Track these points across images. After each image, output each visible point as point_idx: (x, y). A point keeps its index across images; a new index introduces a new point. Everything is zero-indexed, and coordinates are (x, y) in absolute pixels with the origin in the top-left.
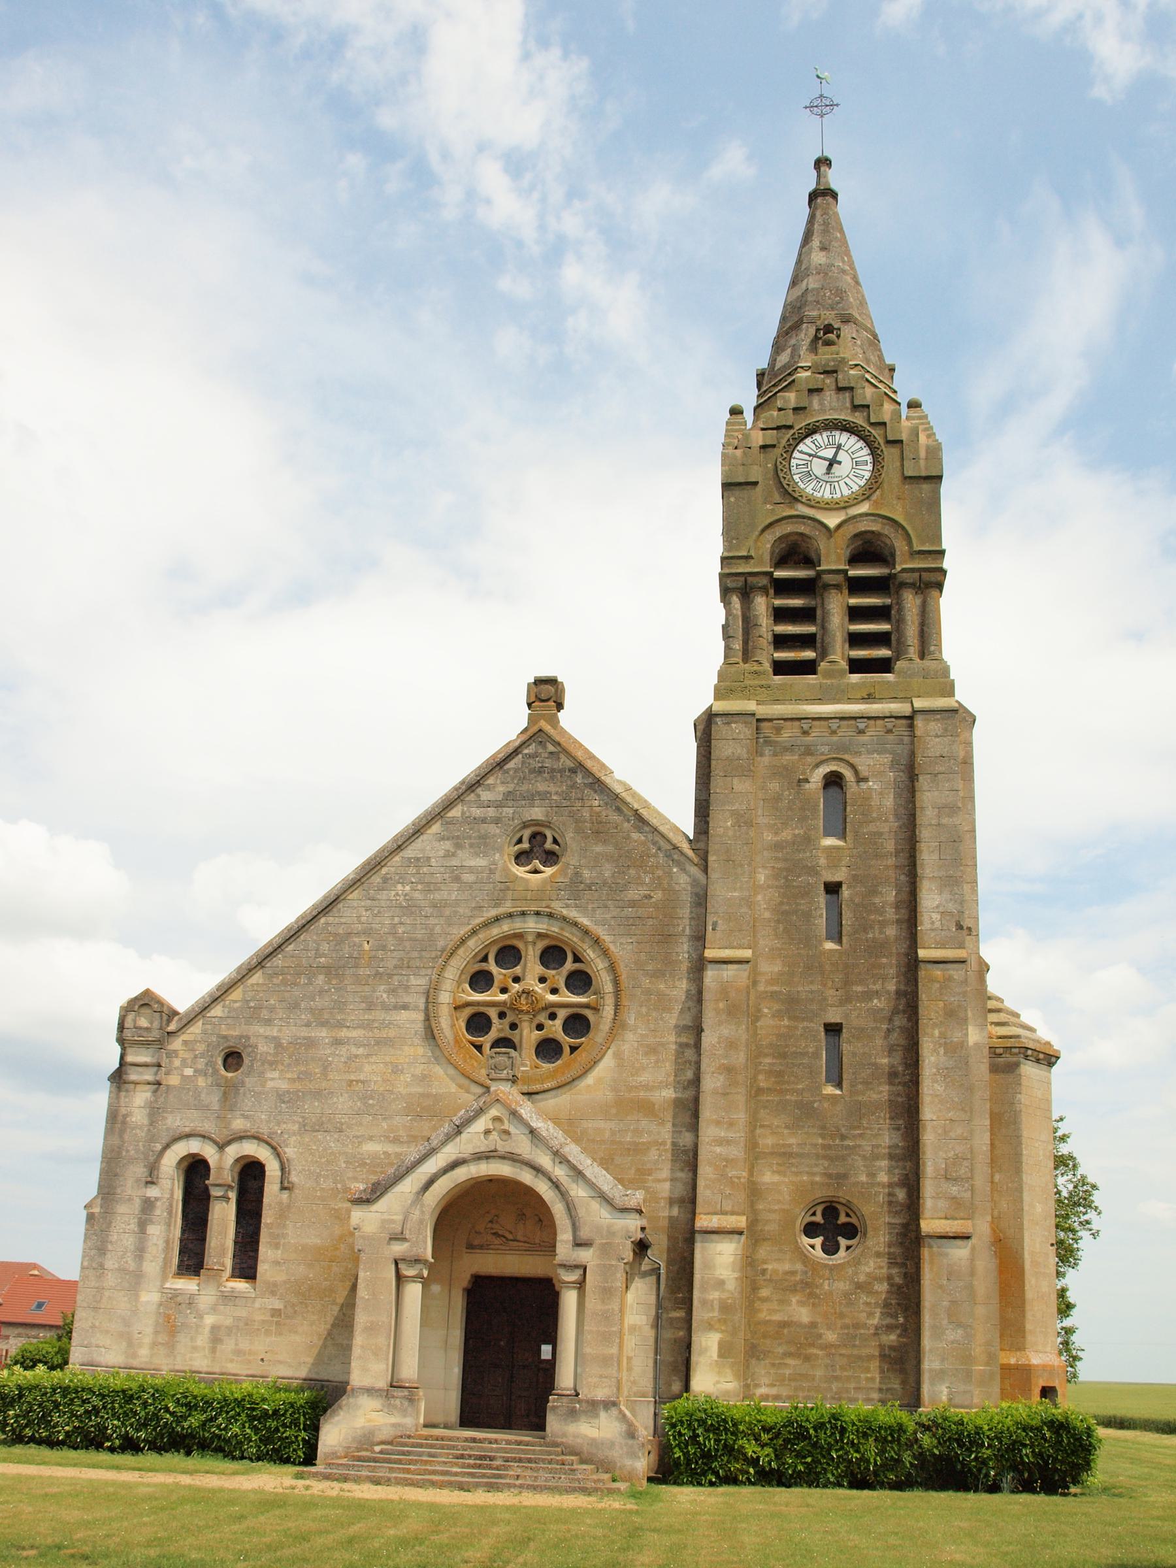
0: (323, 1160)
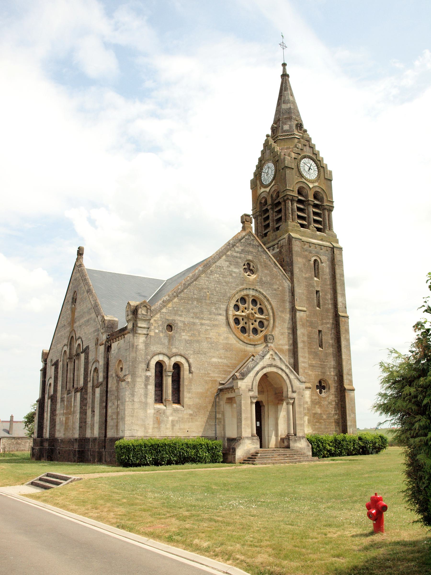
0: (201, 364)
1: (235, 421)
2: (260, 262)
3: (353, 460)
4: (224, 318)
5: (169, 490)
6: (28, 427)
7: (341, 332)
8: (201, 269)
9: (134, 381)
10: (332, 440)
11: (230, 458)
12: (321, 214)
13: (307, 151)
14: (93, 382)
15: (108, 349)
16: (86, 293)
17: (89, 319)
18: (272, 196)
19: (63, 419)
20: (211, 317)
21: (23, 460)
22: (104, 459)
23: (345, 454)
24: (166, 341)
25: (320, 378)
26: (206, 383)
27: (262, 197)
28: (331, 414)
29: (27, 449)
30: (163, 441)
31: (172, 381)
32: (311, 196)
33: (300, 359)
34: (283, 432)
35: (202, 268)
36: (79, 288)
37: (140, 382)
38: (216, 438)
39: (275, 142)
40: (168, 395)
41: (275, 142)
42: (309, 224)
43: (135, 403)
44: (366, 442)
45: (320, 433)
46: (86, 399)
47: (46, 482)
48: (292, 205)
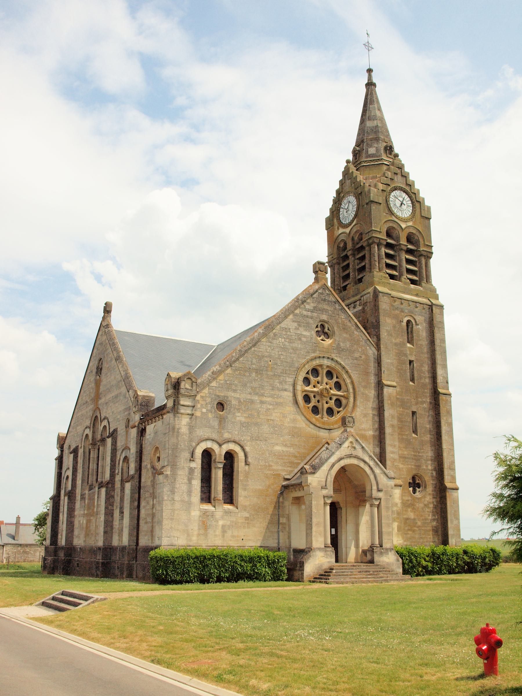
0: (260, 453)
1: (303, 527)
2: (338, 323)
3: (456, 580)
4: (291, 395)
5: (218, 615)
6: (38, 531)
7: (441, 414)
8: (261, 332)
9: (174, 474)
10: (429, 554)
11: (296, 574)
12: (416, 261)
13: (399, 181)
14: (122, 474)
15: (142, 432)
16: (114, 361)
17: (117, 395)
18: (353, 239)
19: (83, 522)
20: (274, 393)
21: (32, 574)
22: (134, 573)
23: (445, 572)
24: (216, 424)
25: (414, 472)
26: (267, 477)
27: (340, 240)
28: (427, 519)
29: (37, 560)
30: (210, 552)
31: (223, 475)
32: (403, 239)
33: (389, 449)
34: (365, 542)
35: (263, 330)
36: (105, 355)
37: (182, 475)
38: (279, 548)
39: (357, 170)
40: (217, 492)
41: (357, 170)
42: (401, 275)
43: (175, 502)
44: (473, 557)
45: (413, 544)
46: (113, 497)
47: (60, 602)
48: (378, 251)
